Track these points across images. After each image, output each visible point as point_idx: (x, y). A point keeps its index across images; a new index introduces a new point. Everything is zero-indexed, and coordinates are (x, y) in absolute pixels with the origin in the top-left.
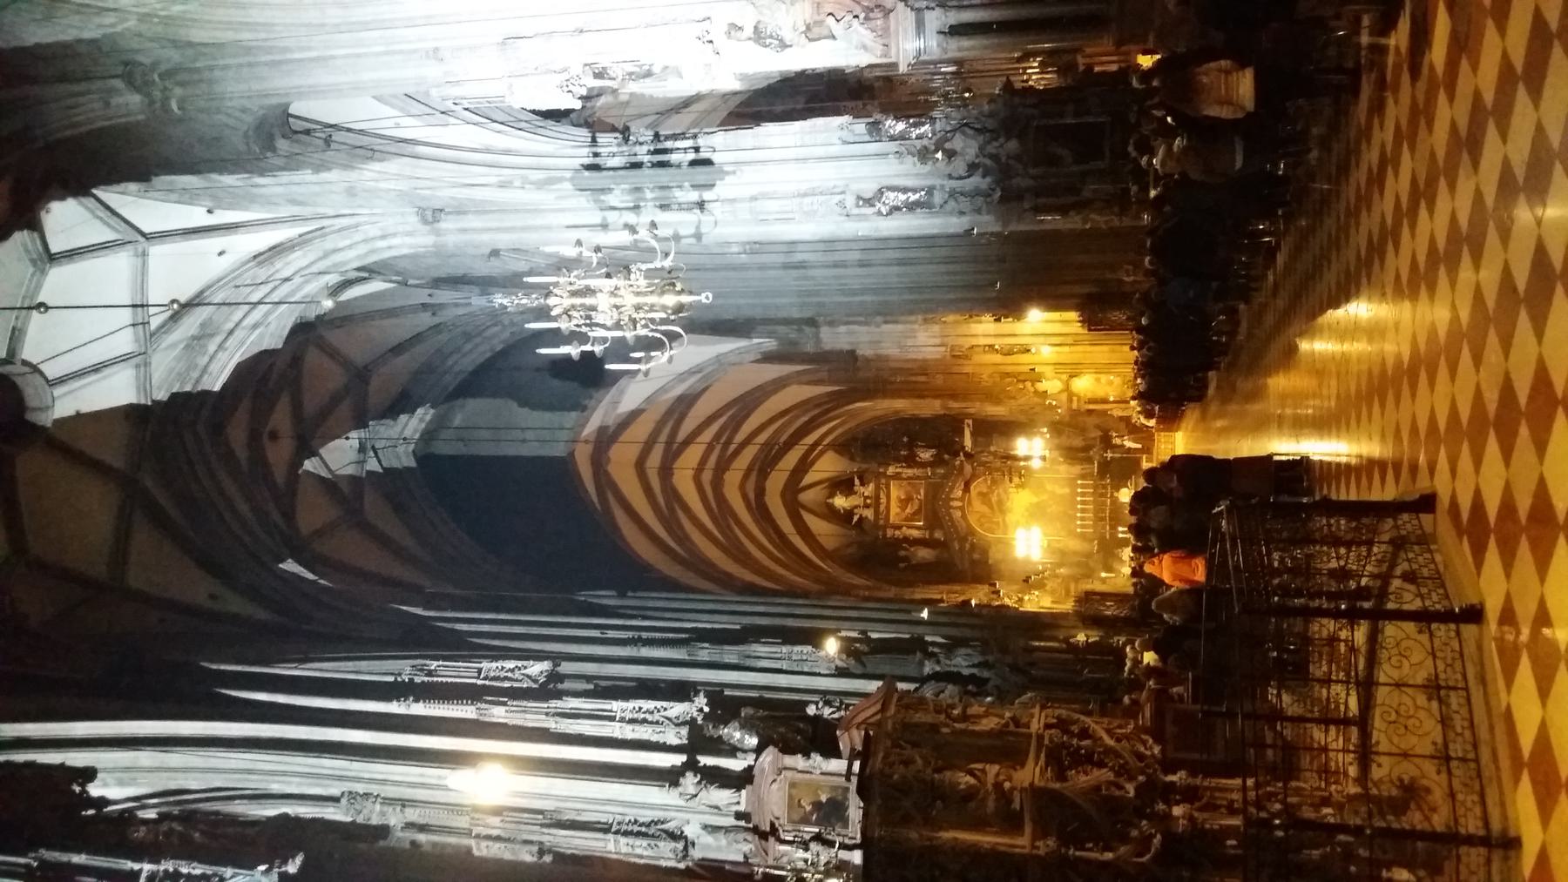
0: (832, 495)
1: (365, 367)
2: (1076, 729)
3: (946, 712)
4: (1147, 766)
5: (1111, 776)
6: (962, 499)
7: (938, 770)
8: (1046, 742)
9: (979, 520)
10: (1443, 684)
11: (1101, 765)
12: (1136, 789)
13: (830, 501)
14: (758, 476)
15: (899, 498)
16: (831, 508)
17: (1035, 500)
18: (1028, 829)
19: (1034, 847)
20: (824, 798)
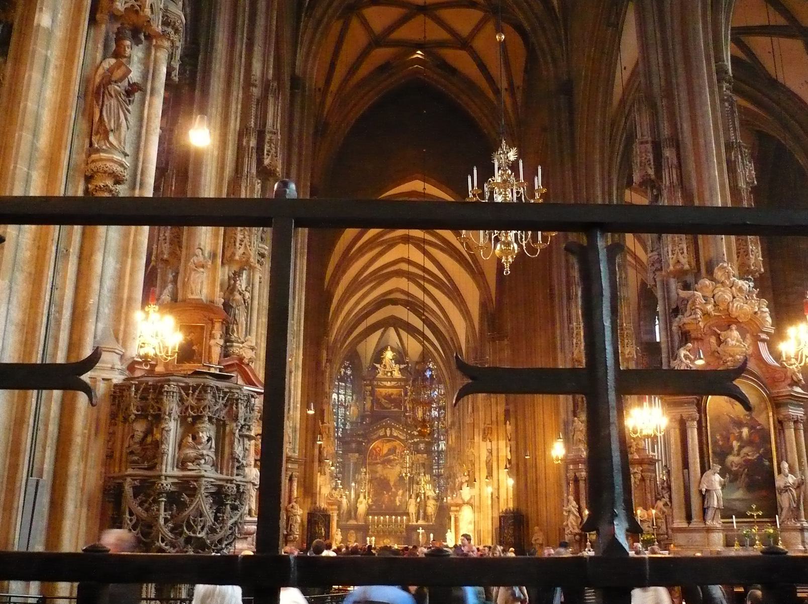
0: (393, 349)
1: (471, 47)
3: (245, 425)
5: (209, 524)
6: (391, 435)
7: (210, 419)
8: (229, 485)
9: (378, 447)
11: (216, 518)
13: (389, 349)
14: (408, 301)
15: (392, 394)
16: (385, 349)
17: (392, 483)
18: (177, 472)
19: (166, 477)
20: (195, 348)
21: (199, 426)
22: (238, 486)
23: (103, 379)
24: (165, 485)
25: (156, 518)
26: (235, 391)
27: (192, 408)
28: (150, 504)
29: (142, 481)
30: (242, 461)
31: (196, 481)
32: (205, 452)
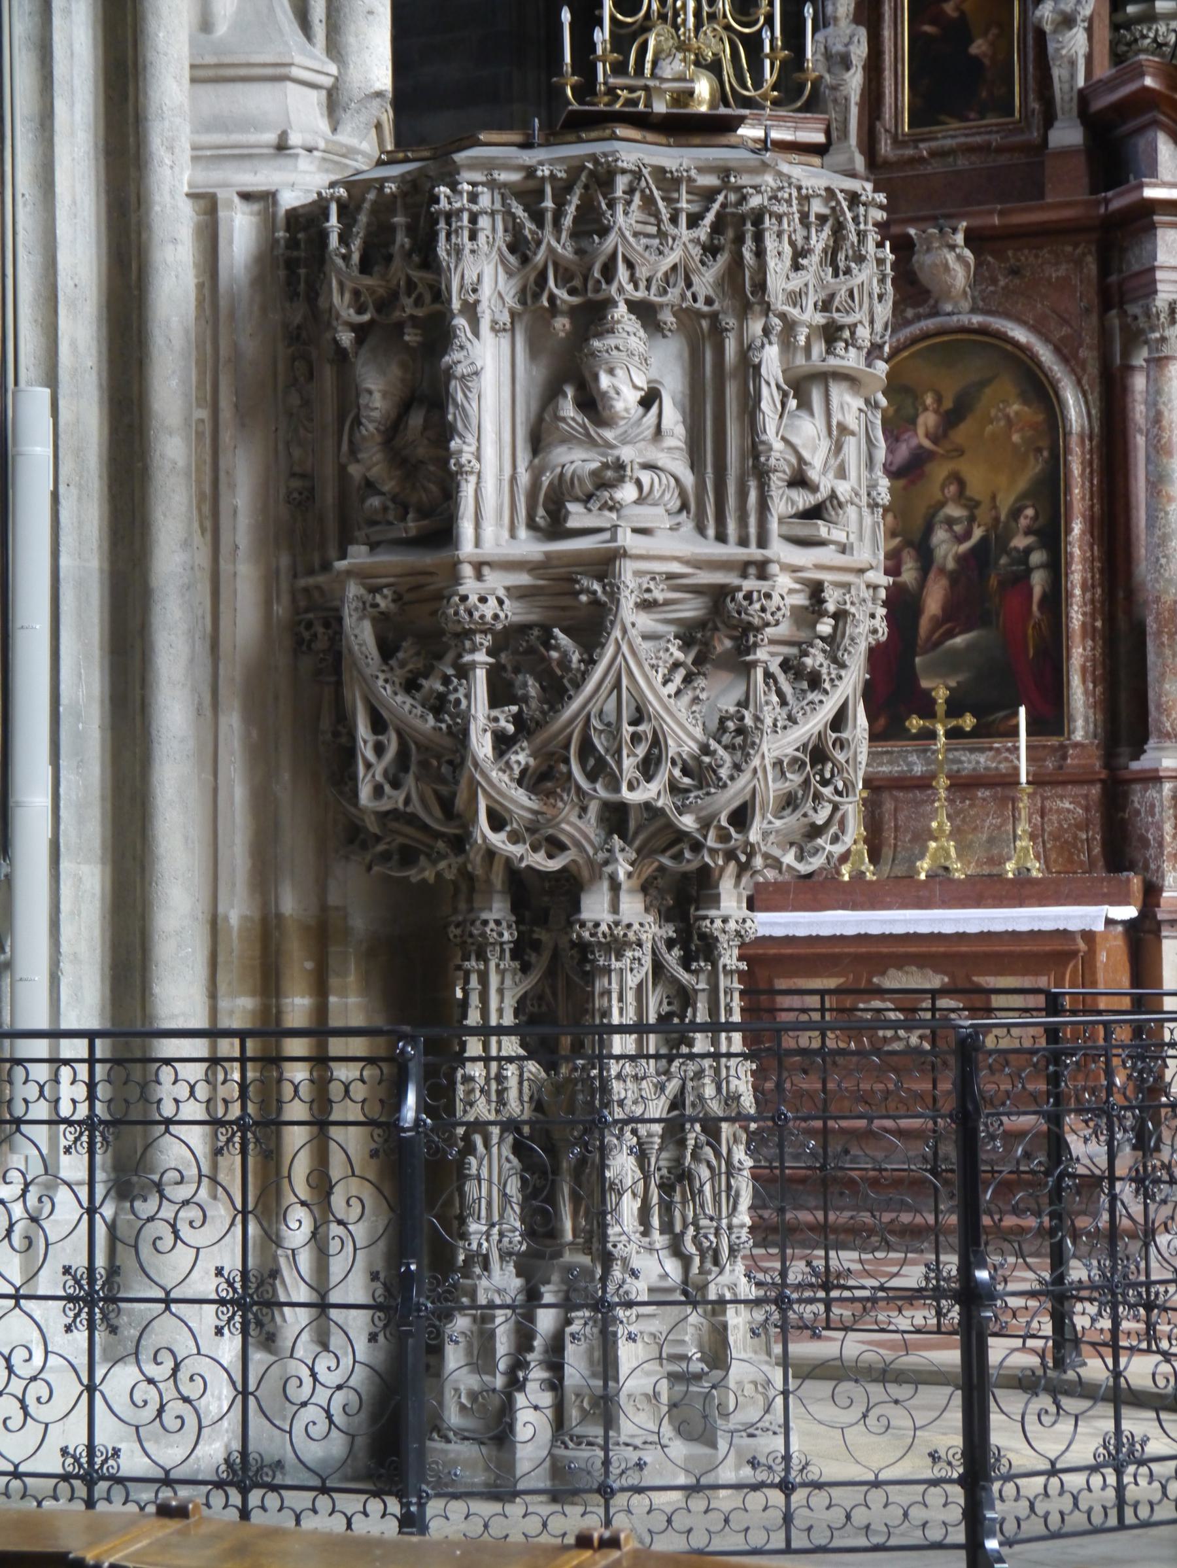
2: (815, 659)
4: (724, 837)
7: (645, 312)
8: (749, 584)
10: (798, 1497)
12: (647, 806)
18: (529, 547)
19: (479, 567)
20: (978, 47)
21: (596, 344)
22: (816, 591)
23: (246, 196)
24: (473, 599)
25: (461, 736)
26: (744, 180)
27: (565, 276)
28: (446, 680)
29: (398, 598)
30: (826, 483)
31: (600, 578)
32: (627, 453)
